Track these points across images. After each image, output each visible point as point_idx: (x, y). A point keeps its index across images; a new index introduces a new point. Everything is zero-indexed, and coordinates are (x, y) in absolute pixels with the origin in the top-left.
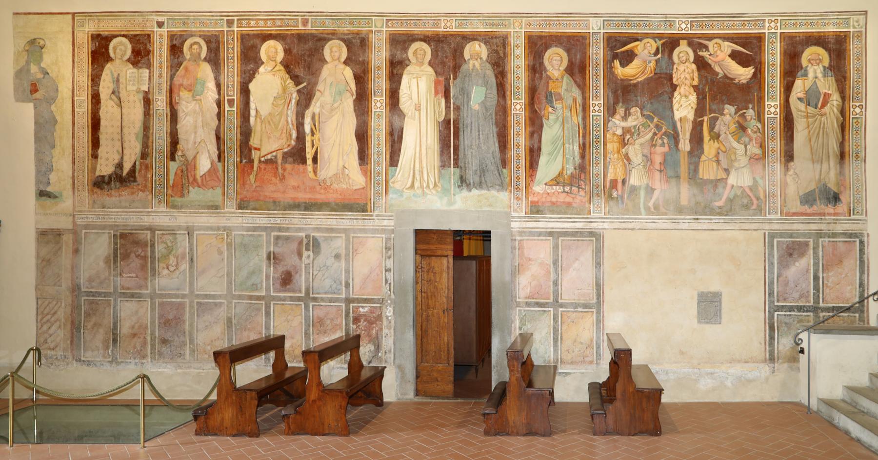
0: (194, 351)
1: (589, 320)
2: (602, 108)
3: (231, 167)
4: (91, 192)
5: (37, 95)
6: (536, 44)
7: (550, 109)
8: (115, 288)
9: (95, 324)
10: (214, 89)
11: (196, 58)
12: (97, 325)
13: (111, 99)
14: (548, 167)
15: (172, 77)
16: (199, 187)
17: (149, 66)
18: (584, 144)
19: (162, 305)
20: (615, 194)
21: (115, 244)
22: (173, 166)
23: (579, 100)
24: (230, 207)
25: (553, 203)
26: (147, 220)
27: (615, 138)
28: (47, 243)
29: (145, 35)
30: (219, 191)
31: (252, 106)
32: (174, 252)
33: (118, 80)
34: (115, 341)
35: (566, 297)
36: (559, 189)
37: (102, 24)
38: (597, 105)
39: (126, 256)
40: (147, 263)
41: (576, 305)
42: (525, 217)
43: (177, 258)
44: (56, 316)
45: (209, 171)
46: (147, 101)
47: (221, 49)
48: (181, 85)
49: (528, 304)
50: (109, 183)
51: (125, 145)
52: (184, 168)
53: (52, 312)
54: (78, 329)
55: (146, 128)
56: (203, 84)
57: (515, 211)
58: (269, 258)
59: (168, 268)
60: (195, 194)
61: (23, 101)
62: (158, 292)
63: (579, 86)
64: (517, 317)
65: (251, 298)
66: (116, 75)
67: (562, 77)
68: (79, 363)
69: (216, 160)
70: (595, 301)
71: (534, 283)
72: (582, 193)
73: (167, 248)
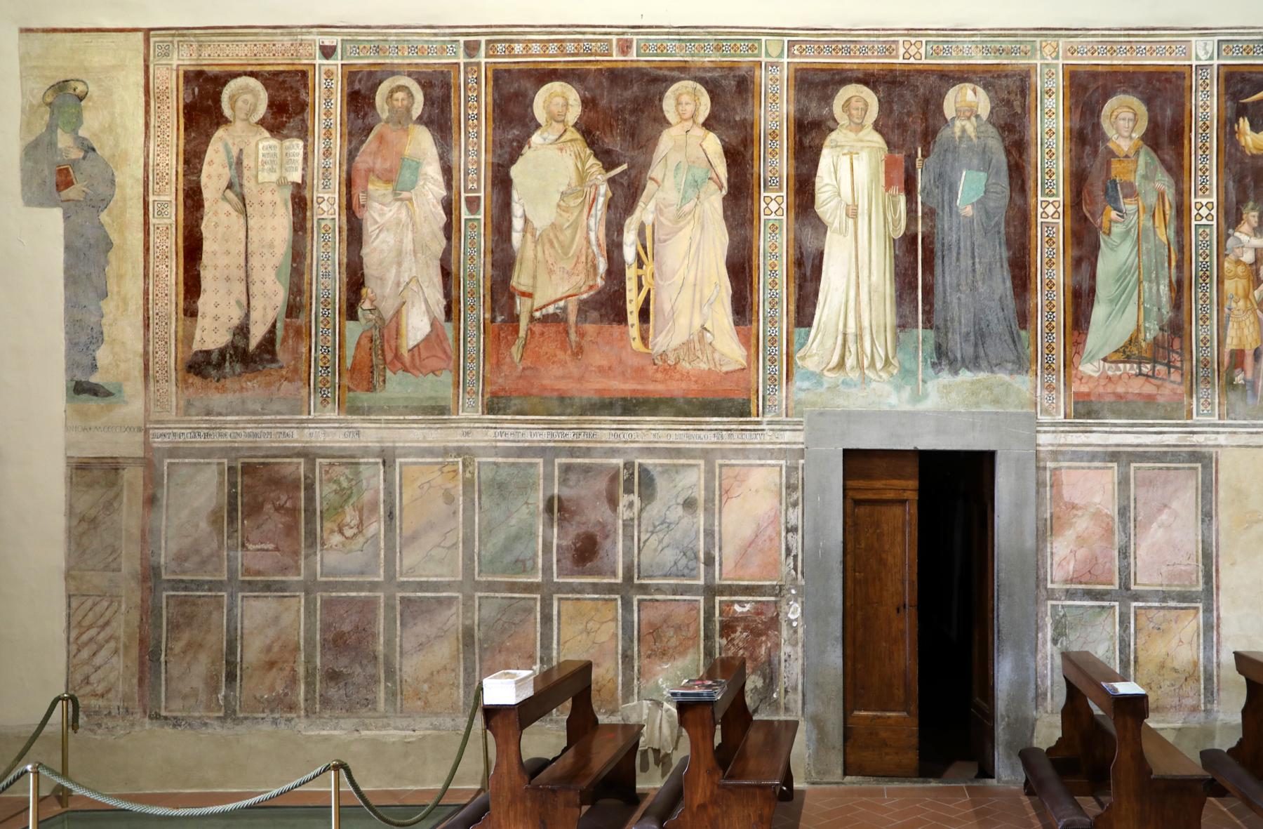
0: (394, 694)
1: (1191, 624)
2: (1214, 212)
3: (472, 331)
4: (183, 383)
5: (71, 193)
6: (1085, 89)
7: (1114, 214)
8: (232, 572)
9: (189, 645)
10: (439, 177)
11: (401, 118)
12: (194, 647)
13: (225, 198)
14: (1111, 324)
15: (351, 156)
16: (406, 370)
17: (304, 133)
18: (1180, 283)
19: (328, 604)
20: (1239, 379)
21: (233, 484)
22: (354, 330)
23: (1170, 196)
24: (470, 410)
25: (1119, 397)
26: (298, 438)
27: (1240, 269)
28: (90, 485)
29: (296, 72)
30: (447, 377)
31: (517, 210)
32: (354, 499)
33: (239, 162)
34: (231, 677)
35: (1144, 580)
36: (1131, 368)
37: (205, 53)
38: (1205, 206)
39: (254, 509)
40: (297, 522)
41: (1165, 596)
42: (1063, 424)
43: (361, 511)
44: (108, 631)
45: (427, 339)
46: (300, 203)
47: (453, 100)
48: (371, 170)
49: (1070, 594)
50: (219, 365)
51: (253, 289)
52: (376, 333)
53: (101, 622)
54: (155, 655)
55: (298, 255)
56: (416, 167)
57: (1046, 411)
58: (549, 508)
59: (341, 532)
60: (397, 386)
61: (41, 205)
62: (319, 578)
63: (1169, 170)
64: (1049, 620)
65: (512, 587)
66: (235, 152)
67: (1137, 153)
68: (156, 723)
69: (442, 317)
70: (1200, 587)
71: (1082, 553)
72: (1176, 376)
73: (340, 492)
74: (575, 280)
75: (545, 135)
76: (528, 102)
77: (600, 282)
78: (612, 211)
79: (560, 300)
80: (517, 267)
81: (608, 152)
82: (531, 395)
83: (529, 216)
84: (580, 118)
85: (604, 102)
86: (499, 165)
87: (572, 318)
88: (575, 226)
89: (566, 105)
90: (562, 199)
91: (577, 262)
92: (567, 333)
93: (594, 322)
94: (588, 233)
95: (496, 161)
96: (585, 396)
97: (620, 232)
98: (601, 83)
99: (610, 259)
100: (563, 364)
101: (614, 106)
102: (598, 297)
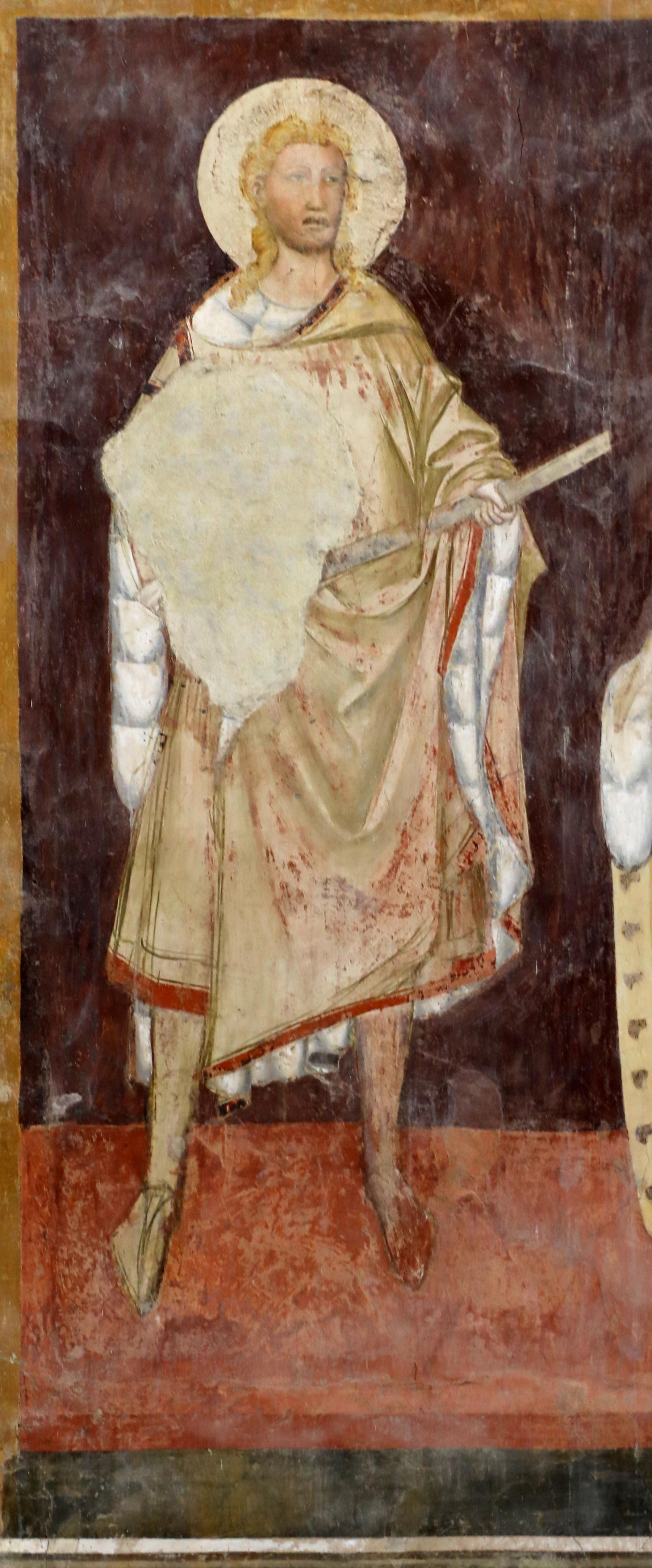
31: (133, 627)
74: (389, 933)
75: (252, 306)
76: (173, 158)
77: (501, 944)
78: (547, 639)
79: (330, 1020)
80: (137, 877)
81: (527, 384)
82: (201, 1444)
83: (186, 656)
84: (401, 237)
85: (502, 169)
86: (50, 432)
87: (383, 1100)
88: (387, 699)
89: (342, 177)
90: (328, 583)
91: (400, 859)
92: (361, 1166)
93: (476, 1120)
94: (444, 731)
95: (37, 414)
96: (446, 1445)
97: (587, 728)
98: (488, 84)
99: (543, 845)
100: (345, 1303)
101: (546, 185)
102: (494, 1009)
